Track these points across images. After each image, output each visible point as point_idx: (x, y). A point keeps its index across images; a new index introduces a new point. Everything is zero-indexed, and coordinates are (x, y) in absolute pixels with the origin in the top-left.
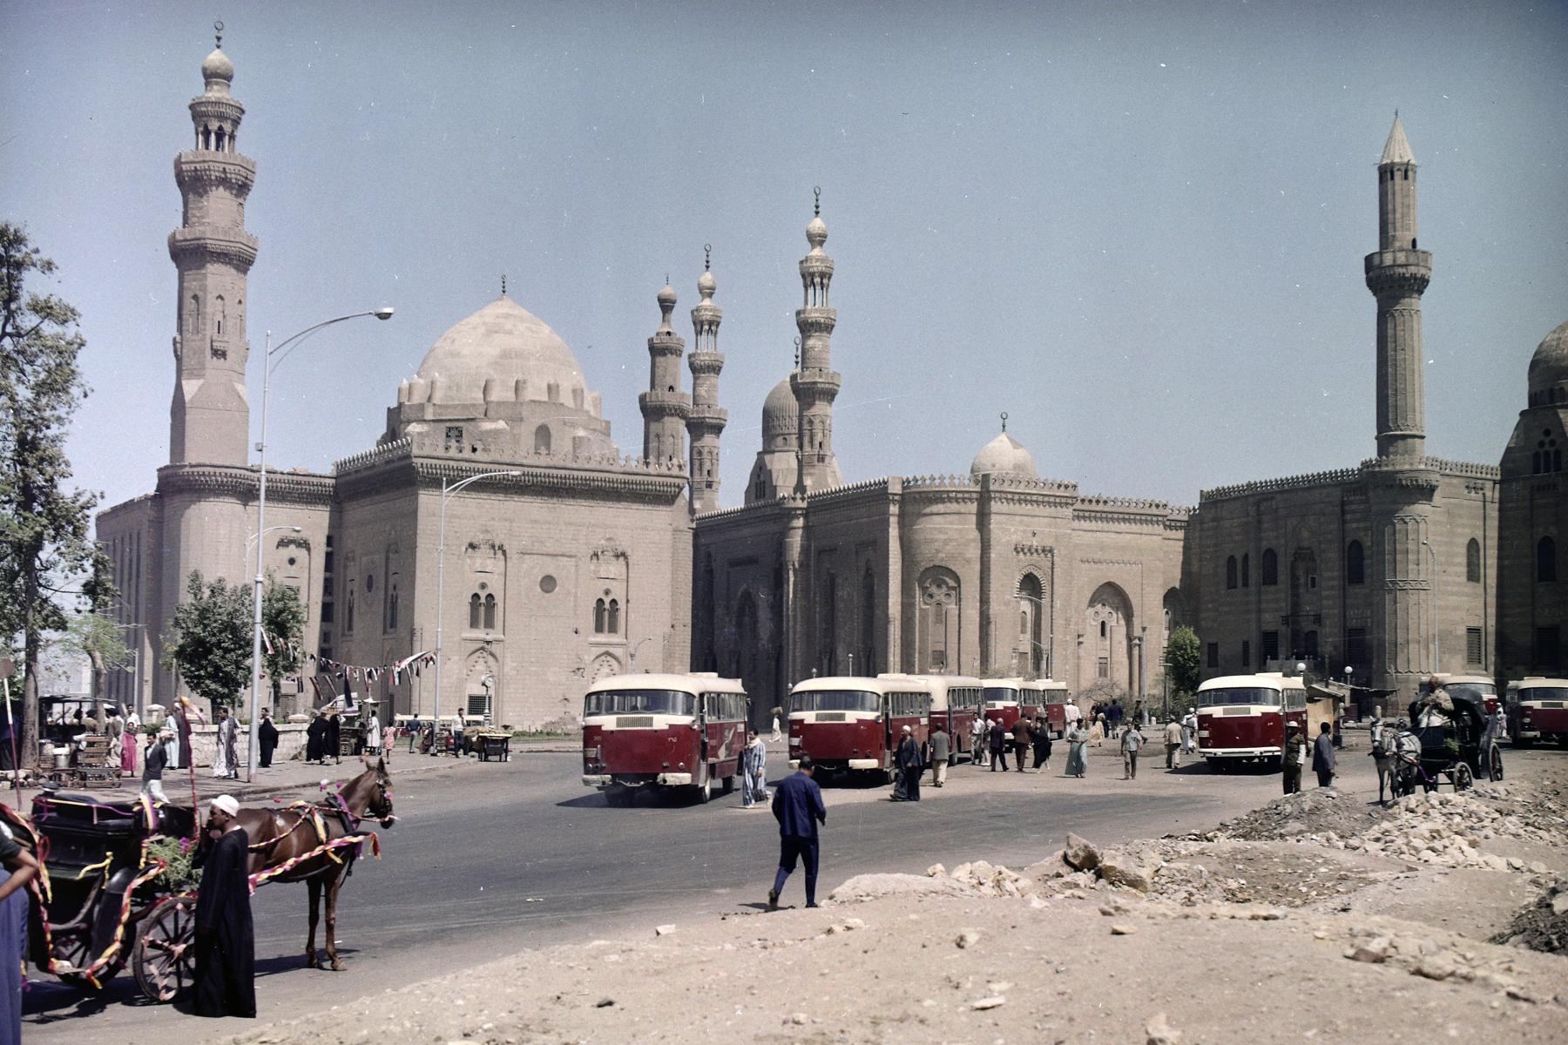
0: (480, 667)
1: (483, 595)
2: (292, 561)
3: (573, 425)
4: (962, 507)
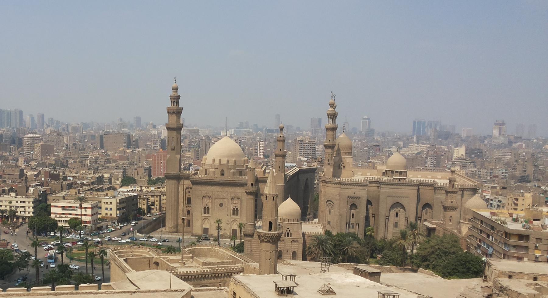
3: (231, 169)
4: (335, 186)
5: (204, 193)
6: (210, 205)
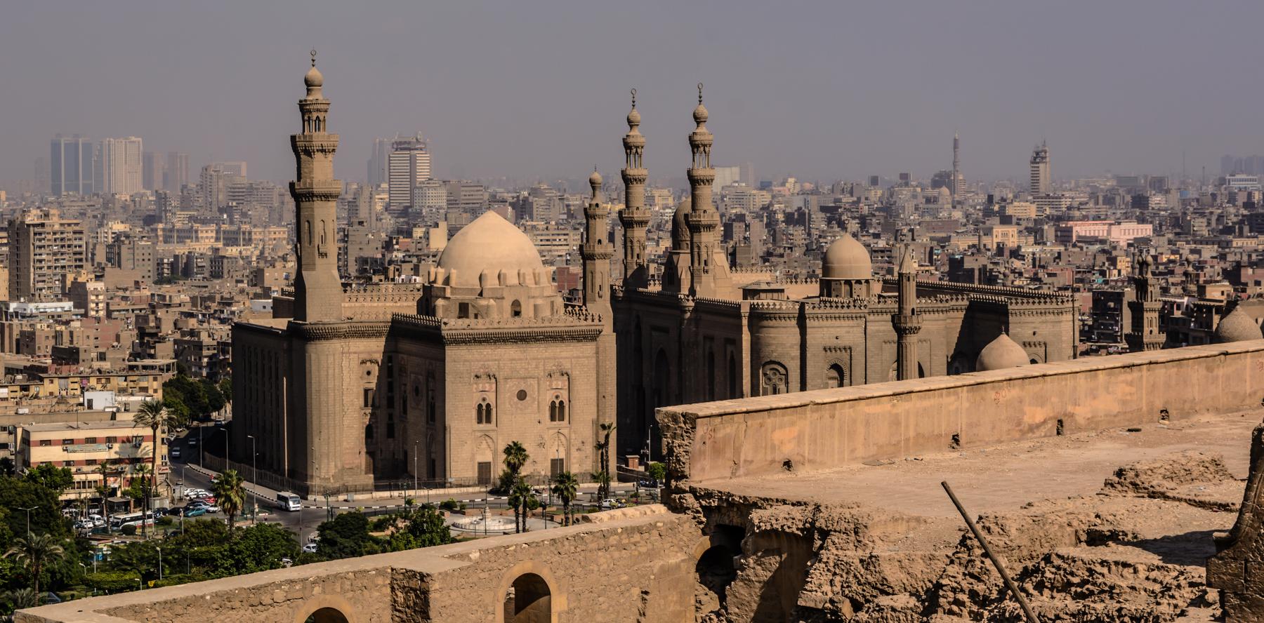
0: (484, 445)
1: (484, 405)
2: (369, 373)
5: (477, 368)
6: (491, 399)
